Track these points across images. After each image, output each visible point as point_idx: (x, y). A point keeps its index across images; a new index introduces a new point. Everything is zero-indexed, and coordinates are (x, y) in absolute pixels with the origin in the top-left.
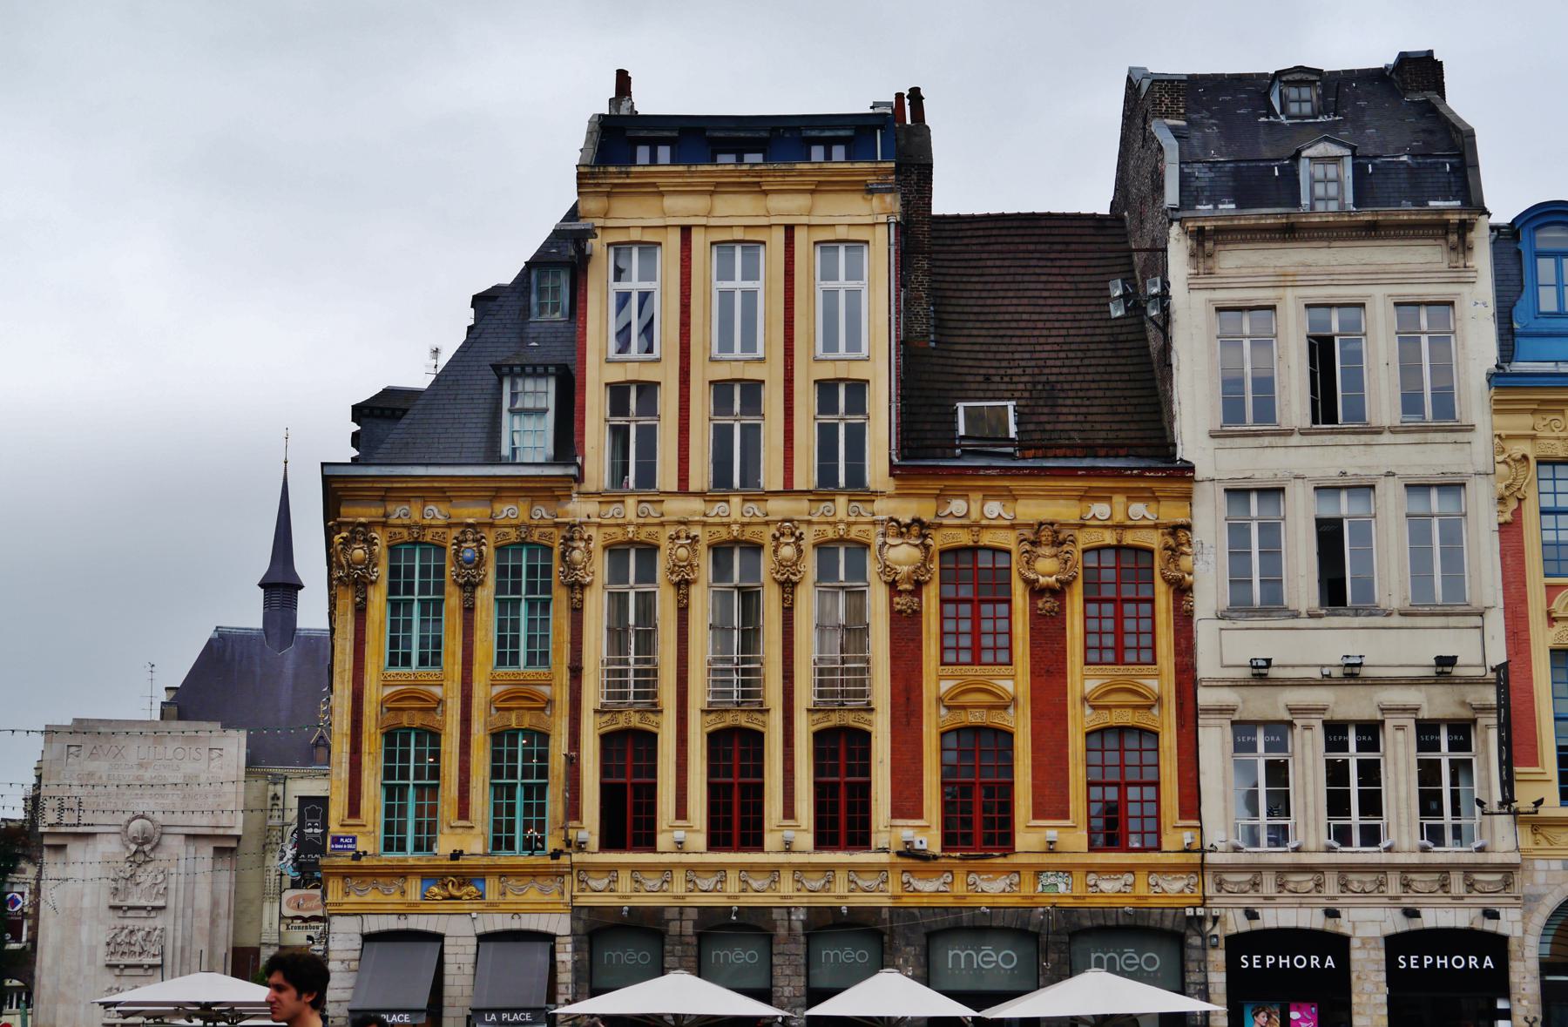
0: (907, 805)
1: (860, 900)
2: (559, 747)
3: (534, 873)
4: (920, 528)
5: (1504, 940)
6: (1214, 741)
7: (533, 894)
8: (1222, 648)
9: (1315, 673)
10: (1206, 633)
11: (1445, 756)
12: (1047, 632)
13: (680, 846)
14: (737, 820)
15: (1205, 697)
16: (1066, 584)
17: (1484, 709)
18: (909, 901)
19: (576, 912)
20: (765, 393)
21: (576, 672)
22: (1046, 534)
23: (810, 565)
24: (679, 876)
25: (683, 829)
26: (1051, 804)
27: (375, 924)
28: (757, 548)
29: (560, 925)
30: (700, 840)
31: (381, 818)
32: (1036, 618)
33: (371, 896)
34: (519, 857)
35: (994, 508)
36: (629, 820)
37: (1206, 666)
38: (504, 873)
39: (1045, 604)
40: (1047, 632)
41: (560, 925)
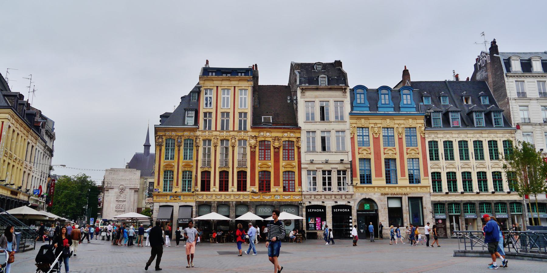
0: (253, 184)
1: (207, 200)
2: (194, 174)
3: (189, 195)
4: (256, 137)
5: (325, 207)
6: (304, 173)
7: (189, 199)
8: (305, 158)
9: (321, 162)
10: (303, 155)
11: (327, 176)
12: (277, 155)
13: (214, 191)
14: (224, 187)
15: (303, 166)
16: (280, 147)
17: (348, 168)
18: (253, 200)
19: (196, 202)
20: (213, 114)
21: (197, 161)
22: (277, 138)
23: (219, 142)
24: (214, 196)
25: (215, 188)
26: (277, 184)
27: (162, 204)
28: (228, 140)
29: (193, 204)
30: (218, 190)
31: (163, 186)
32: (275, 152)
33: (161, 199)
34: (187, 192)
35: (268, 134)
36: (205, 186)
37: (303, 161)
38: (184, 195)
39: (276, 150)
40: (277, 155)
41: (193, 204)
